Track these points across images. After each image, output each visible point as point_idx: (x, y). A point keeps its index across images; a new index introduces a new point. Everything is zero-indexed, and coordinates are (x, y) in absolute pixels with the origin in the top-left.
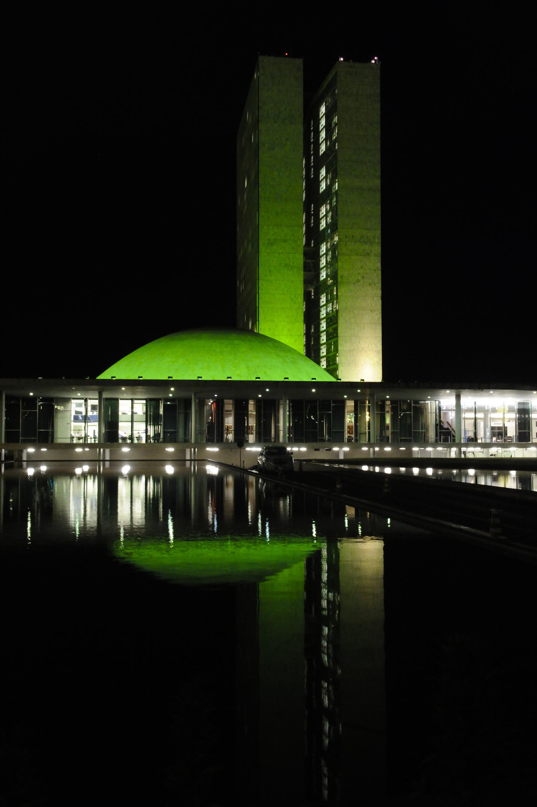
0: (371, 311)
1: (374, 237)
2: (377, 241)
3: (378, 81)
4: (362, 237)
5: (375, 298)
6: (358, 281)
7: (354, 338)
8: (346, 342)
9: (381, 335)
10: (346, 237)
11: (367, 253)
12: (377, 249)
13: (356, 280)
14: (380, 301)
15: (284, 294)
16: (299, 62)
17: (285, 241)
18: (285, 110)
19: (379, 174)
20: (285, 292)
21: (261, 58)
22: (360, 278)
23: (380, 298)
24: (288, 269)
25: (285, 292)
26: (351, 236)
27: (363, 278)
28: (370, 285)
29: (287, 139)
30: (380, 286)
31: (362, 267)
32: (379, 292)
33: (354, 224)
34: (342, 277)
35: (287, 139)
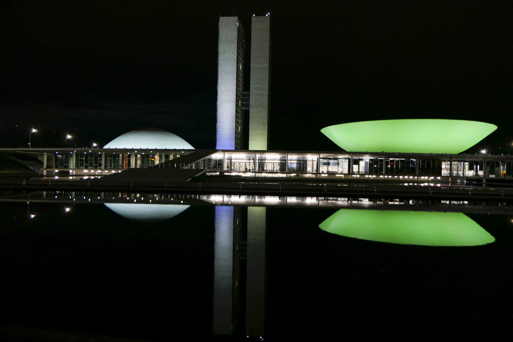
3: (269, 23)
12: (266, 93)
16: (236, 18)
17: (228, 91)
19: (268, 62)
21: (220, 17)
32: (267, 111)
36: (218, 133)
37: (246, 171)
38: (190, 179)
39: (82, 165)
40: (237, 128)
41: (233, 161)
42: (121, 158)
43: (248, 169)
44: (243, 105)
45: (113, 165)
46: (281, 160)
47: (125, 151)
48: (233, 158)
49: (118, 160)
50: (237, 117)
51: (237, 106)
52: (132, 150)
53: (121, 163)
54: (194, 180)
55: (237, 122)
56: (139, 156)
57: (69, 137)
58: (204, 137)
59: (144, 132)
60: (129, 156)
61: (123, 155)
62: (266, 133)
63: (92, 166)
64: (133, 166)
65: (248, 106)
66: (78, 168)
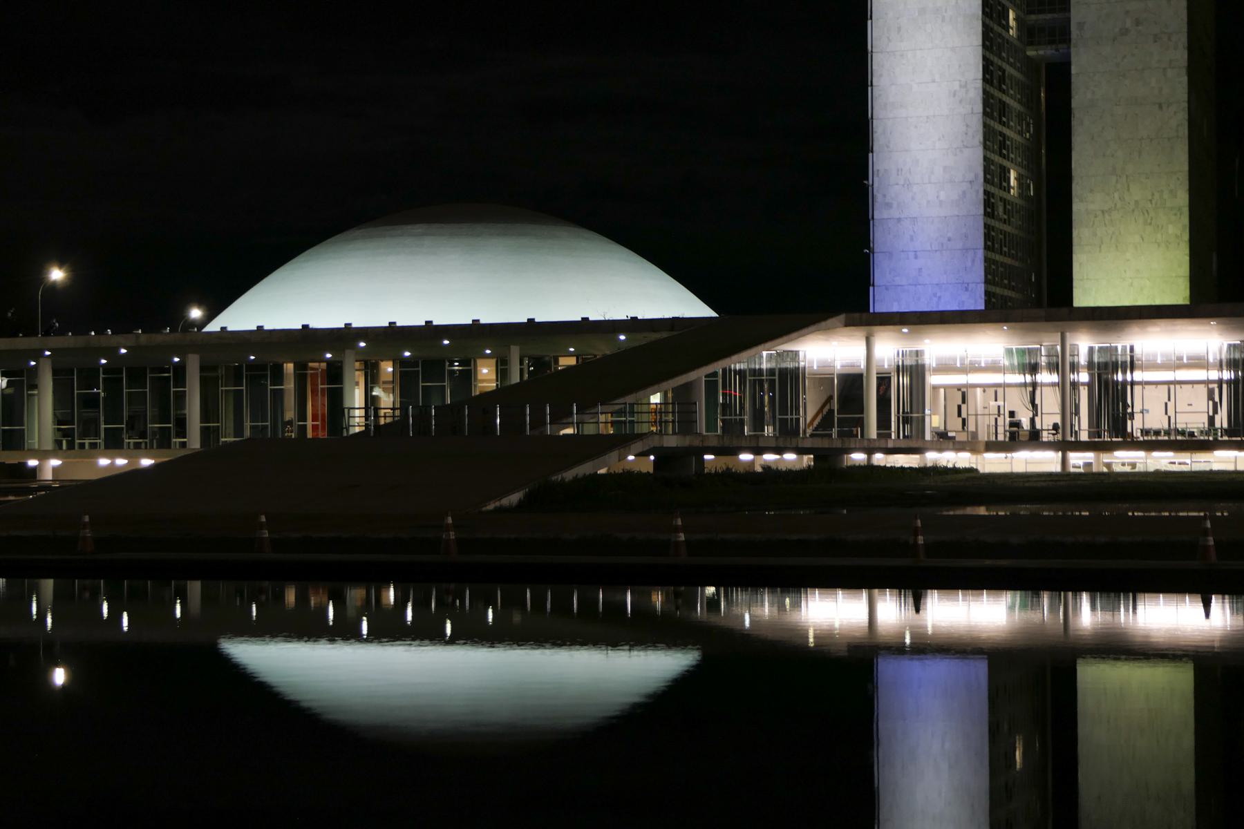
0: (1160, 106)
5: (1170, 73)
6: (1125, 32)
7: (1114, 179)
8: (1091, 191)
9: (1186, 168)
13: (1117, 30)
14: (1185, 79)
15: (934, 81)
20: (937, 78)
22: (1129, 23)
23: (1184, 72)
24: (943, 20)
25: (937, 78)
27: (1138, 23)
28: (1156, 38)
30: (1183, 39)
32: (1180, 56)
34: (1081, 25)
36: (880, 213)
37: (1020, 437)
38: (514, 498)
39: (89, 428)
40: (993, 175)
41: (933, 380)
42: (289, 386)
43: (1026, 424)
44: (1029, 33)
45: (248, 424)
46: (1233, 364)
47: (308, 339)
48: (929, 359)
49: (279, 396)
50: (992, 108)
51: (991, 41)
52: (344, 337)
53: (290, 414)
54: (545, 498)
55: (993, 141)
56: (388, 368)
57: (57, 275)
58: (794, 235)
59: (419, 228)
60: (335, 374)
61: (301, 367)
62: (1183, 198)
63: (143, 435)
64: (357, 421)
65: (1061, 35)
66: (71, 446)
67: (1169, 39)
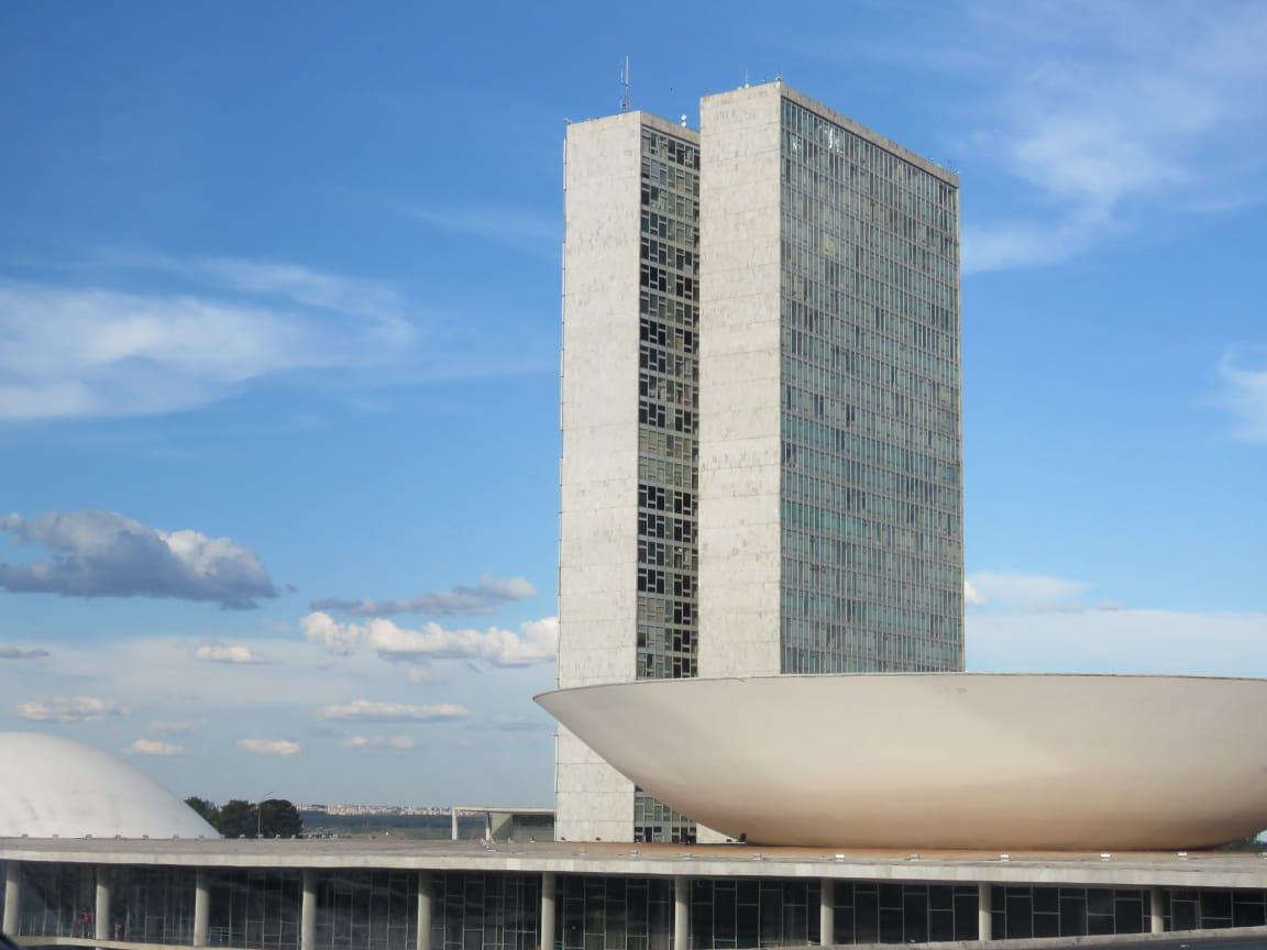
0: (760, 614)
1: (766, 453)
2: (772, 461)
4: (743, 457)
10: (715, 460)
11: (754, 490)
17: (606, 484)
18: (610, 218)
22: (739, 545)
26: (724, 458)
27: (745, 544)
28: (758, 557)
29: (612, 278)
31: (743, 521)
33: (728, 430)
35: (612, 278)
67: (768, 557)
